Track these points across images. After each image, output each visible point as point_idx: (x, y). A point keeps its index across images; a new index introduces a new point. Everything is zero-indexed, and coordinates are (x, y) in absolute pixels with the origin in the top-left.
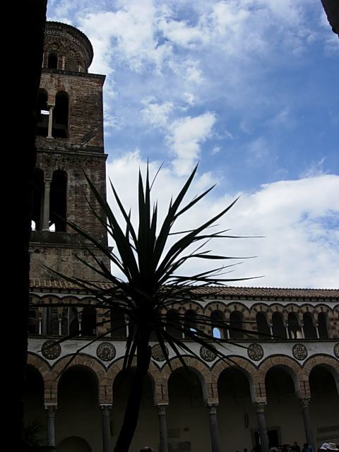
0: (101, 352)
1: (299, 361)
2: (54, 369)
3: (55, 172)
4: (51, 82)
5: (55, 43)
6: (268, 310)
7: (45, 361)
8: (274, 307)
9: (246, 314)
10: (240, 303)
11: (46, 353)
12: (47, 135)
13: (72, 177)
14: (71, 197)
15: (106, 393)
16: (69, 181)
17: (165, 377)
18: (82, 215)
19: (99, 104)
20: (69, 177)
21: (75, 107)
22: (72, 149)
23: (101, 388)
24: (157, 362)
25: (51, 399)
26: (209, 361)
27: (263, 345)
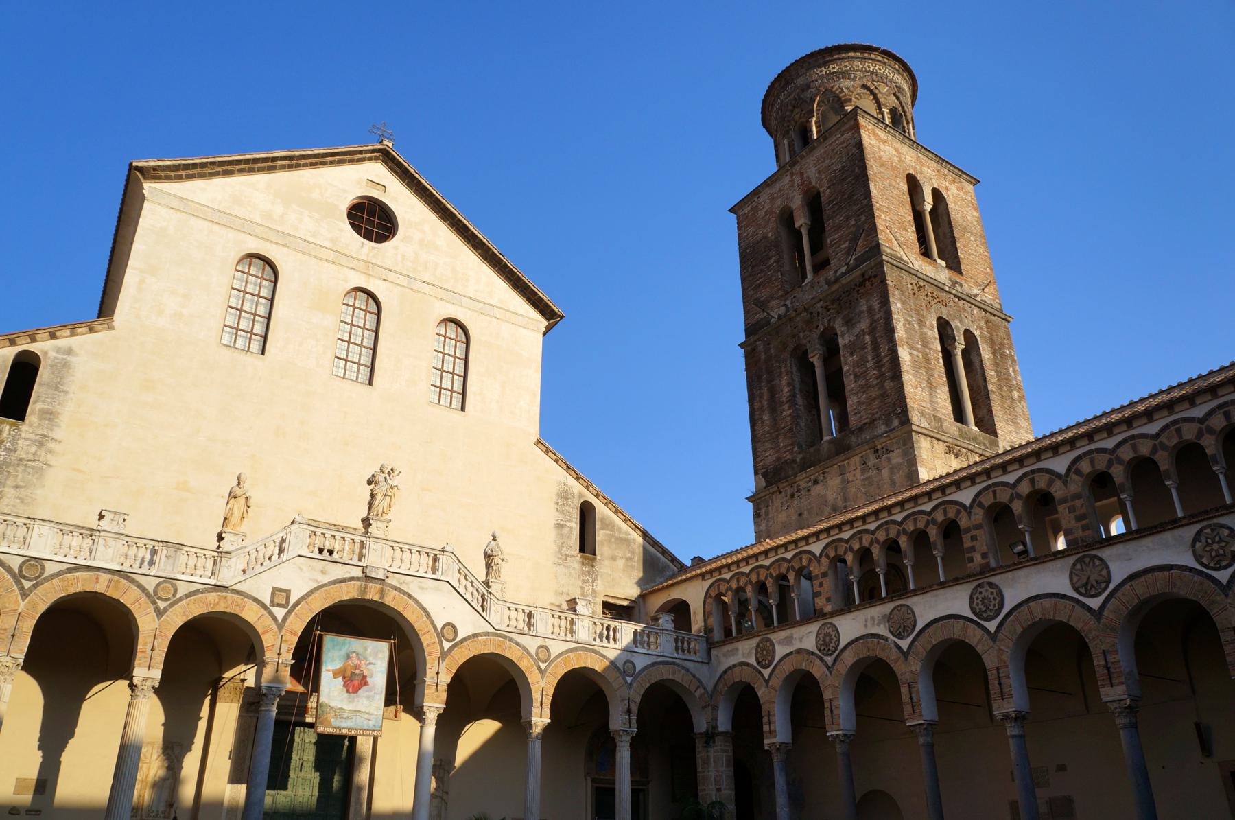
0: (821, 642)
1: (1215, 574)
2: (770, 684)
3: (823, 334)
4: (793, 186)
5: (794, 107)
6: (1110, 460)
7: (760, 672)
8: (1127, 447)
9: (1058, 491)
10: (1040, 471)
11: (760, 660)
12: (806, 277)
13: (843, 329)
14: (848, 365)
15: (831, 711)
16: (840, 340)
17: (913, 668)
18: (865, 388)
19: (859, 169)
20: (839, 333)
21: (829, 203)
22: (837, 280)
23: (827, 705)
24: (899, 641)
25: (770, 732)
26: (989, 619)
27: (1106, 553)
